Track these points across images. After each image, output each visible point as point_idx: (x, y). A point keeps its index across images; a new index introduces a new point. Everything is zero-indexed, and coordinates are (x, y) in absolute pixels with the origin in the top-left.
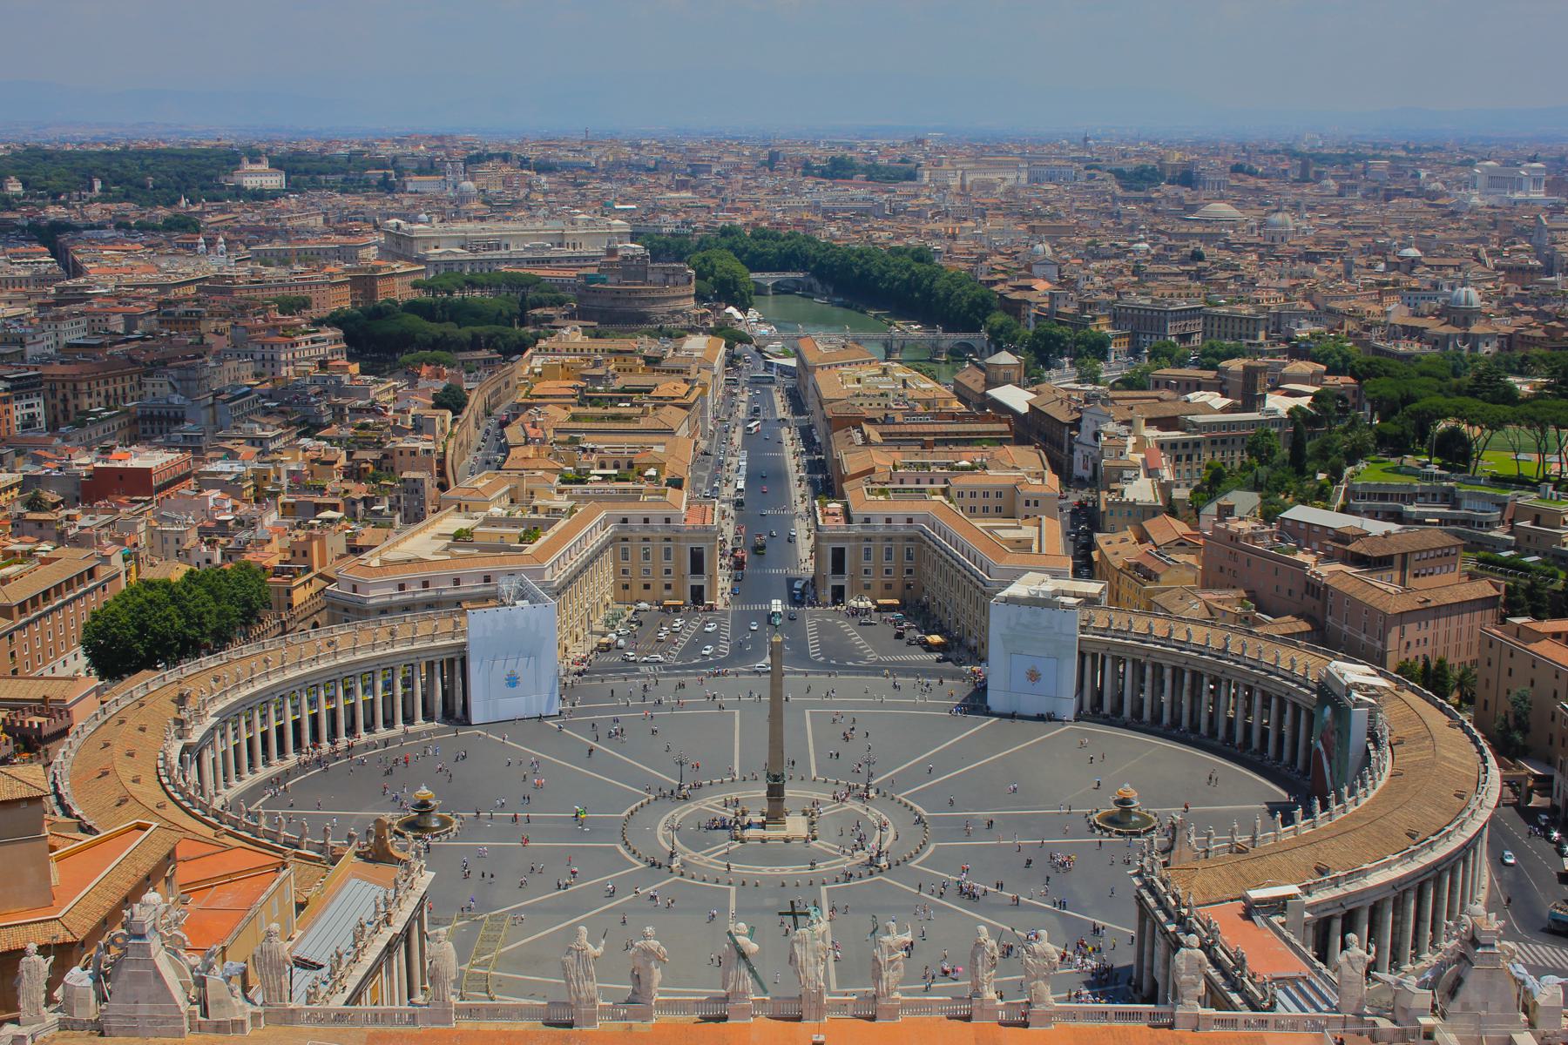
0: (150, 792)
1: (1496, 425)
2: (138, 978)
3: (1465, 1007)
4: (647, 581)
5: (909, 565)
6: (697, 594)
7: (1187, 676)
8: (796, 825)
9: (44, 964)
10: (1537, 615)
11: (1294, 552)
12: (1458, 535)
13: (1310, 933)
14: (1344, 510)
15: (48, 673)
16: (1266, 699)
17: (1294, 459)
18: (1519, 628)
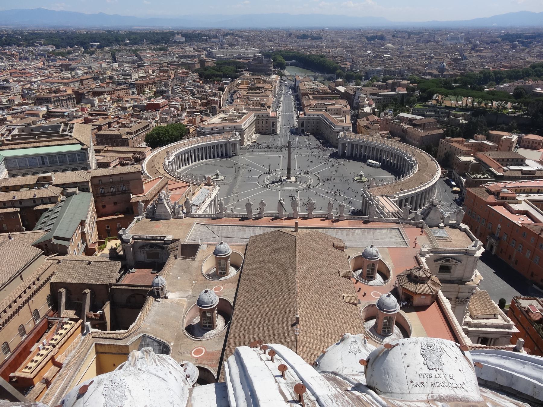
0: (162, 171)
1: (446, 95)
3: (430, 218)
8: (293, 179)
9: (143, 204)
10: (453, 137)
12: (436, 119)
13: (398, 202)
14: (411, 114)
16: (392, 154)
17: (402, 103)
18: (448, 140)
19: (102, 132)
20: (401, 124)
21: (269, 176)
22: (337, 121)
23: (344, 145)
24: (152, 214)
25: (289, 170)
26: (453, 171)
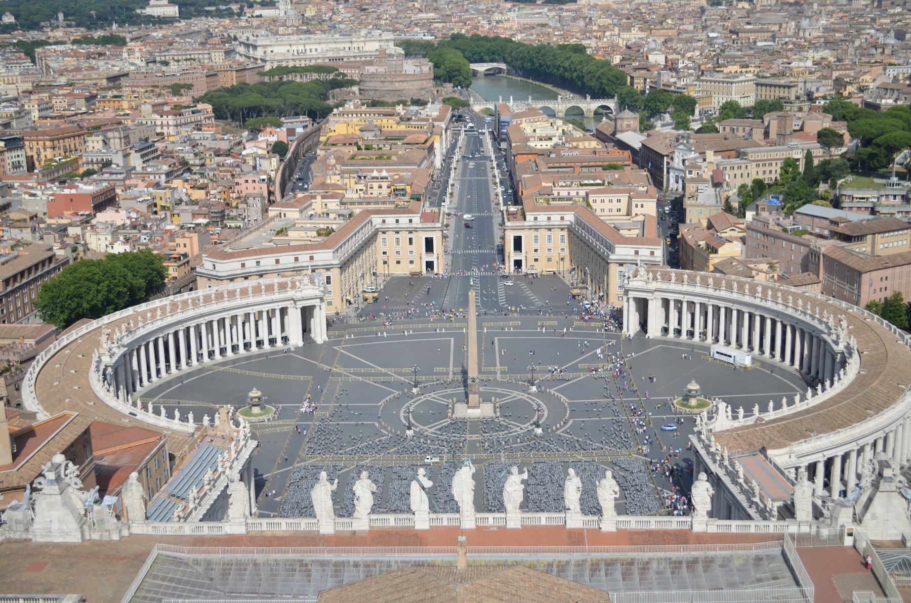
2: (51, 506)
4: (398, 258)
6: (430, 265)
7: (735, 313)
14: (836, 203)
24: (21, 527)
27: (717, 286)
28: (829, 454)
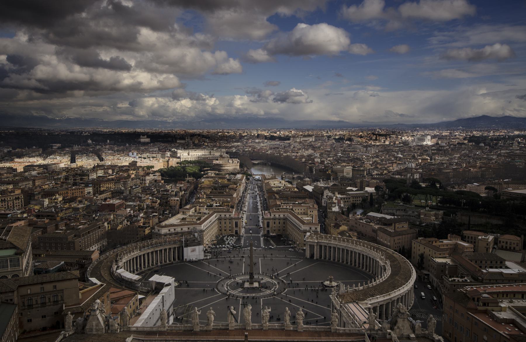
1: (416, 194)
3: (398, 328)
5: (284, 225)
11: (370, 223)
14: (381, 213)
15: (88, 250)
19: (46, 235)
20: (371, 224)
21: (229, 282)
22: (303, 222)
23: (312, 247)
25: (251, 275)
26: (430, 275)
27: (339, 240)
28: (381, 303)
